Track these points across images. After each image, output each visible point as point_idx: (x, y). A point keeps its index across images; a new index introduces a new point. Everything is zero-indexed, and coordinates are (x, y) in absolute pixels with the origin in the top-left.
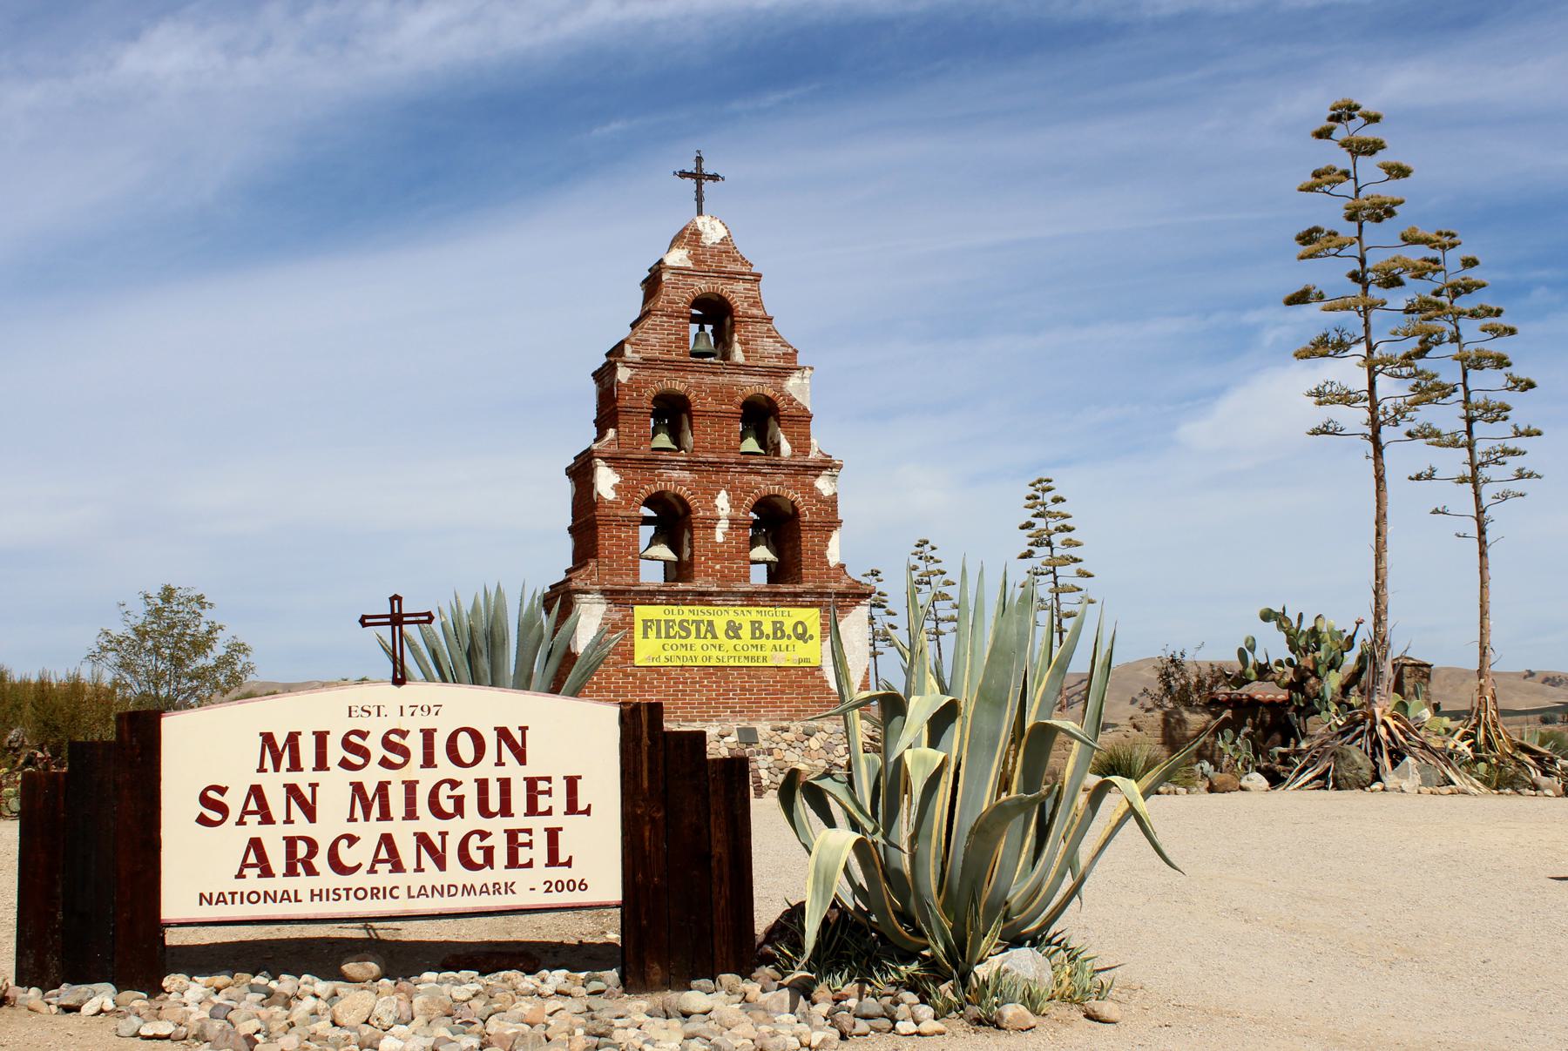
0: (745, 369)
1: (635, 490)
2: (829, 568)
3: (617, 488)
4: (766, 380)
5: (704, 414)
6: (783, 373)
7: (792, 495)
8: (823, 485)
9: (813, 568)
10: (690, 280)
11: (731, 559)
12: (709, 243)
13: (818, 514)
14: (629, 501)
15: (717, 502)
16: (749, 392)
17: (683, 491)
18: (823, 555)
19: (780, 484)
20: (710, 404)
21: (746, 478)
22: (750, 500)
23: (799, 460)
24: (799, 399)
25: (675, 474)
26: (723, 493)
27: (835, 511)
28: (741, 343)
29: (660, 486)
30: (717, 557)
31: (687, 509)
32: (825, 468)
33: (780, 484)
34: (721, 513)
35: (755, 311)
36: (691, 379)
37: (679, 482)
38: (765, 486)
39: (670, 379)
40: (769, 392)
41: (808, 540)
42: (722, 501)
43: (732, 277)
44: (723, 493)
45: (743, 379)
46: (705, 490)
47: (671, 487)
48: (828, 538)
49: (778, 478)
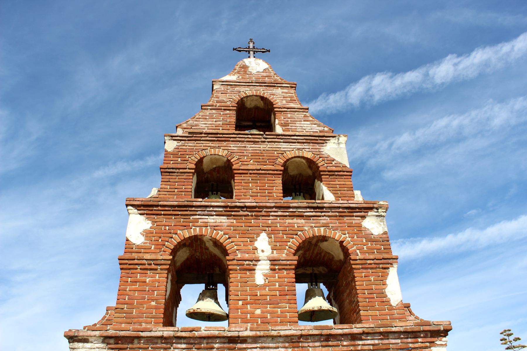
0: (286, 138)
1: (170, 234)
2: (391, 308)
3: (147, 234)
4: (306, 146)
5: (245, 172)
6: (320, 139)
7: (338, 235)
8: (373, 225)
9: (373, 308)
10: (237, 89)
11: (274, 303)
12: (254, 72)
13: (370, 251)
14: (160, 246)
15: (256, 244)
16: (289, 155)
17: (220, 235)
18: (382, 294)
19: (326, 226)
20: (252, 165)
21: (289, 221)
22: (294, 242)
23: (342, 203)
24: (338, 159)
25: (211, 220)
26: (263, 236)
27: (388, 249)
28: (281, 125)
29: (195, 231)
30: (257, 301)
31: (225, 252)
32: (371, 209)
33: (326, 226)
34: (260, 255)
35: (292, 105)
36: (233, 147)
37: (215, 227)
38: (310, 228)
39: (214, 148)
40: (309, 155)
41: (362, 280)
42: (263, 244)
43: (272, 85)
44: (263, 236)
45: (284, 146)
46: (244, 234)
47: (207, 232)
48: (385, 276)
49: (324, 220)
